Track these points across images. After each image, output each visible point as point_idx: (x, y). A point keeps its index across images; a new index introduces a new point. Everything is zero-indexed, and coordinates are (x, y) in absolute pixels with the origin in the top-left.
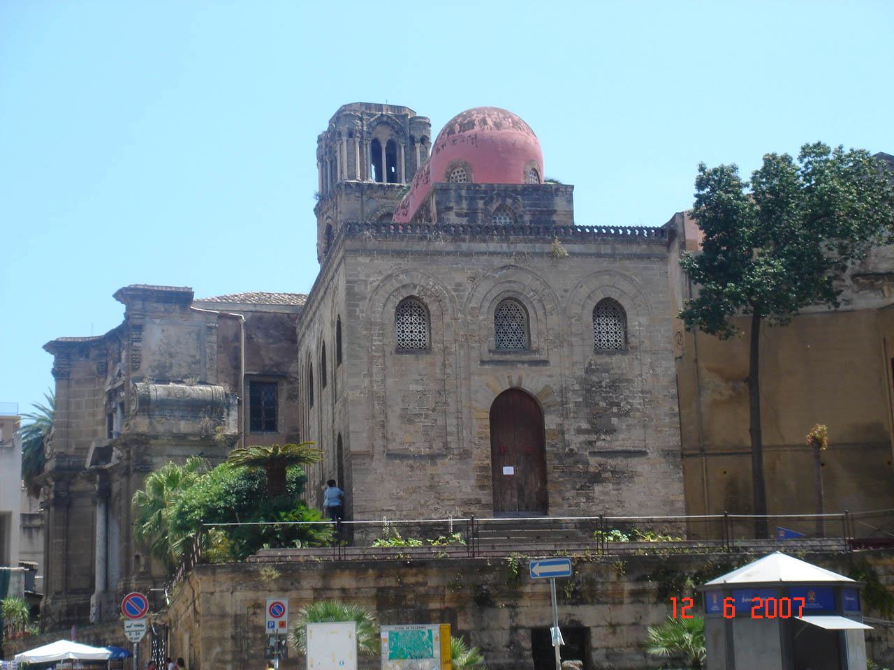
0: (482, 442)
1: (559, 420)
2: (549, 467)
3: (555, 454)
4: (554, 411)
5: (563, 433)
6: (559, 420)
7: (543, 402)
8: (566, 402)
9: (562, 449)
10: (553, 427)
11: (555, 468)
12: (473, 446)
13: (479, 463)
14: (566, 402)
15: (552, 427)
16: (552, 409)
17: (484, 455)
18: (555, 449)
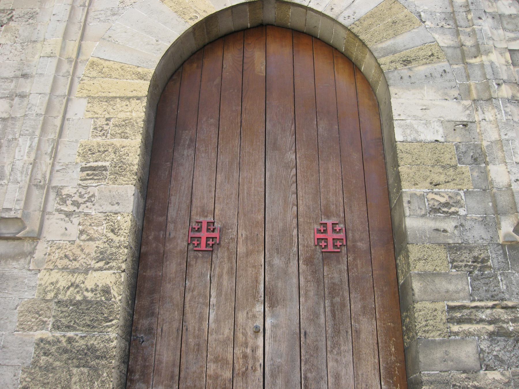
0: (94, 188)
1: (456, 111)
2: (427, 310)
3: (451, 248)
4: (430, 77)
5: (479, 158)
6: (456, 111)
7: (383, 46)
8: (477, 46)
9: (484, 222)
10: (432, 133)
11: (457, 314)
12: (53, 204)
13: (63, 280)
14: (477, 46)
15: (428, 136)
16: (421, 69)
17: (92, 247)
18: (449, 225)
